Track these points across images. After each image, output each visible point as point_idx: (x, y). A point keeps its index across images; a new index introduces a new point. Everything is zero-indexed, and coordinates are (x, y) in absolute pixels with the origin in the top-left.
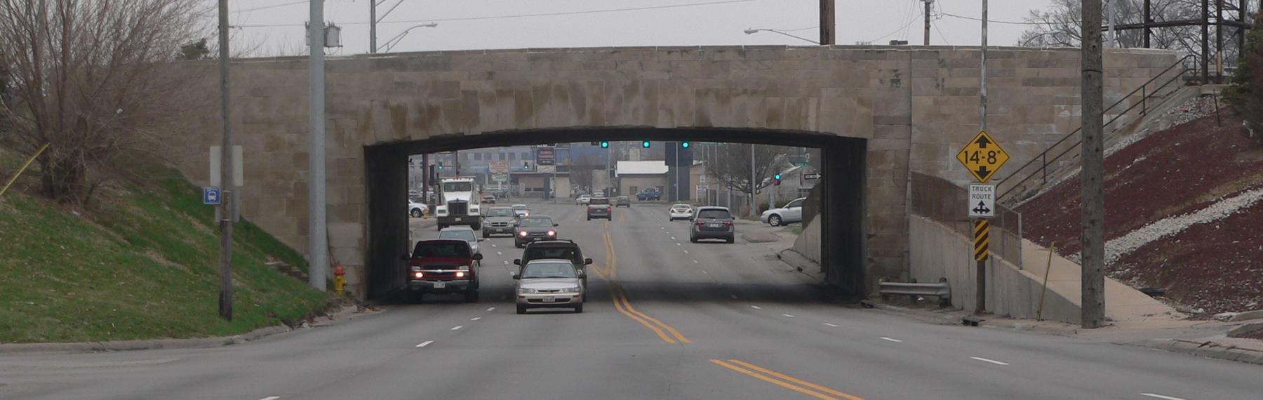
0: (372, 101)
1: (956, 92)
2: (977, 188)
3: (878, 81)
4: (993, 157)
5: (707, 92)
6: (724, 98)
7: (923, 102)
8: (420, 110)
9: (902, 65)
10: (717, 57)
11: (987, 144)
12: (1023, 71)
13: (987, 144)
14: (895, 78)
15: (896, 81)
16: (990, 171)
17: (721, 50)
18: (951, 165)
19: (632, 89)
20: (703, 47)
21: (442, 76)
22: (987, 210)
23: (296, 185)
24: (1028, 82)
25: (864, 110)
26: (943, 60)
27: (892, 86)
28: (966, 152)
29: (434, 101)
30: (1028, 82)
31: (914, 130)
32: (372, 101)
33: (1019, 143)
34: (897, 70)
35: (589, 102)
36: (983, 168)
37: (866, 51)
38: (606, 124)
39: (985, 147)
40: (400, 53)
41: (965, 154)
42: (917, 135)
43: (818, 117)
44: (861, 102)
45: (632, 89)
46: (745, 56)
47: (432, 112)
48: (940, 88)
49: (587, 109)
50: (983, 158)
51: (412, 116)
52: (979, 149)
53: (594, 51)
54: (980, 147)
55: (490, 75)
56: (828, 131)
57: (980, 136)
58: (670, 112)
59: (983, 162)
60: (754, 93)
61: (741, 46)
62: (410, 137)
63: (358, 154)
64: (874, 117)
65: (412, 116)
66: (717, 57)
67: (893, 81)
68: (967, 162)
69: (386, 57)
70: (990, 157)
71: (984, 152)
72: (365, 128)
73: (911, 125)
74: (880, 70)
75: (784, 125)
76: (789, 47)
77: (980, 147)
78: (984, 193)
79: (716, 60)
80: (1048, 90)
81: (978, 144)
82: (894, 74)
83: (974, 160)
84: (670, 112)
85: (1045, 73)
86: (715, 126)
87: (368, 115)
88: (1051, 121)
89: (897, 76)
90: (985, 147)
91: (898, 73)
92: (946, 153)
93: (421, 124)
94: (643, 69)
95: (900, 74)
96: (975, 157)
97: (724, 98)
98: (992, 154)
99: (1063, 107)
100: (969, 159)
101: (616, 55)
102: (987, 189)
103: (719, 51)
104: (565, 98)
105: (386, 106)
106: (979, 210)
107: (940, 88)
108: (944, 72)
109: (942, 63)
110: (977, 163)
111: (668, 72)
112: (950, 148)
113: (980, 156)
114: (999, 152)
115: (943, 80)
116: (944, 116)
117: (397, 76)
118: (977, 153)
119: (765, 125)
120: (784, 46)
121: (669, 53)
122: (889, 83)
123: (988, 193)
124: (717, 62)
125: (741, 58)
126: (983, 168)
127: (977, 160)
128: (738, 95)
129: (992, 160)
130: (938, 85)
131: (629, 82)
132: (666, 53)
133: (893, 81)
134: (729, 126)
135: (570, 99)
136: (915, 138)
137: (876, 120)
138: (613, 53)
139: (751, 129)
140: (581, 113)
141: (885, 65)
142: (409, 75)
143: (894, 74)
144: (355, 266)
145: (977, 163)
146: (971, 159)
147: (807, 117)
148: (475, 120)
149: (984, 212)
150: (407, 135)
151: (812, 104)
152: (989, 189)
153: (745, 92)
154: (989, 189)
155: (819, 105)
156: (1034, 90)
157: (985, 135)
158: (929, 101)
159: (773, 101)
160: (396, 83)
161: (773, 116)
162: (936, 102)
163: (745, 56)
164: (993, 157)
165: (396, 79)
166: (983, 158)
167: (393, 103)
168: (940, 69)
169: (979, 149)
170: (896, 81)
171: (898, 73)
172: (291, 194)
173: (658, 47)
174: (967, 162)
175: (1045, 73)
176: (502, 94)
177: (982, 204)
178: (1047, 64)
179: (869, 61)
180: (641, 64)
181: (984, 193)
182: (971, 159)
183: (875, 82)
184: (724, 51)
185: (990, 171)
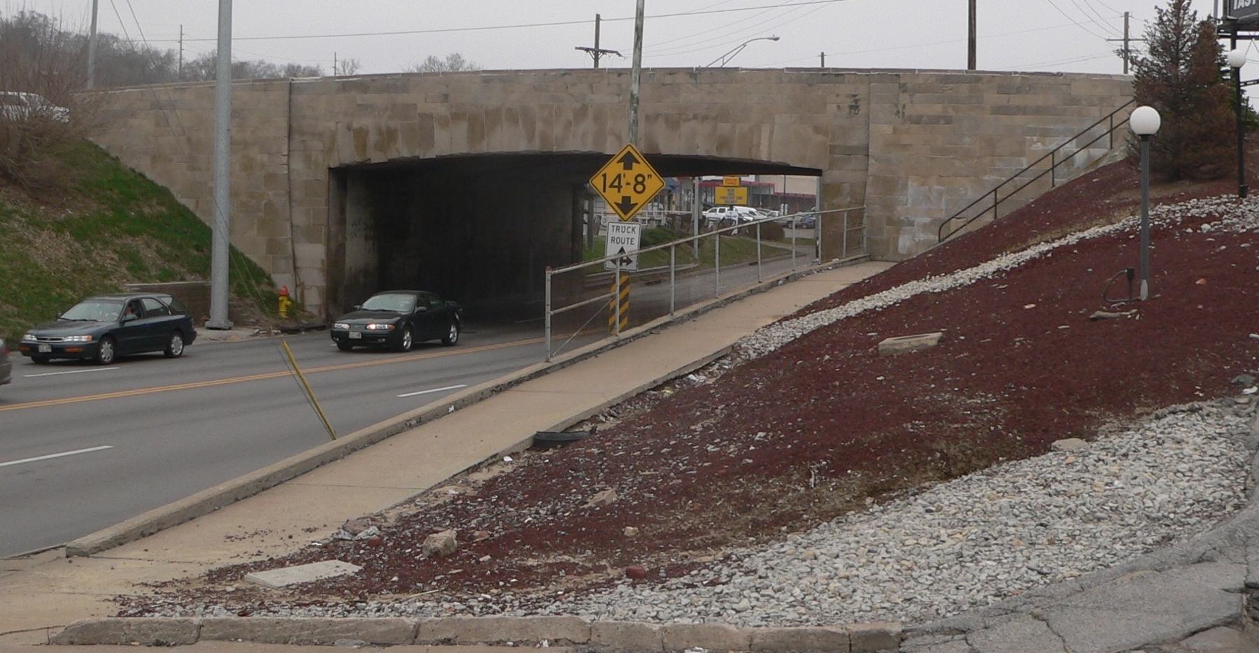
0: (337, 123)
1: (918, 120)
2: (618, 229)
3: (835, 106)
4: (642, 183)
5: (657, 116)
6: (673, 124)
7: (882, 130)
8: (380, 132)
9: (862, 90)
10: (668, 80)
11: (634, 164)
12: (992, 98)
13: (634, 164)
14: (854, 104)
15: (855, 108)
16: (636, 204)
17: (672, 72)
18: (910, 200)
19: (581, 113)
20: (653, 69)
21: (402, 98)
22: (629, 261)
23: (265, 205)
24: (998, 110)
25: (819, 138)
26: (904, 84)
27: (850, 113)
28: (604, 176)
29: (394, 124)
30: (998, 110)
31: (871, 161)
32: (337, 123)
33: (986, 178)
34: (856, 96)
35: (539, 126)
36: (626, 199)
37: (823, 75)
38: (555, 149)
39: (630, 168)
40: (364, 76)
41: (603, 178)
42: (874, 166)
43: (770, 146)
44: (817, 129)
45: (581, 113)
46: (696, 79)
47: (389, 136)
48: (901, 115)
49: (537, 134)
50: (628, 184)
51: (372, 138)
52: (622, 172)
53: (545, 73)
54: (625, 168)
55: (446, 97)
56: (780, 160)
57: (625, 152)
58: (619, 138)
59: (627, 191)
60: (705, 118)
61: (692, 68)
62: (370, 159)
63: (323, 176)
64: (830, 146)
65: (372, 138)
66: (668, 80)
67: (851, 107)
68: (604, 191)
69: (351, 79)
70: (638, 183)
71: (630, 176)
72: (329, 151)
73: (868, 155)
74: (838, 96)
75: (735, 153)
76: (743, 69)
77: (625, 168)
78: (626, 235)
79: (666, 82)
80: (1019, 119)
81: (622, 164)
82: (852, 99)
83: (615, 187)
84: (619, 138)
85: (1016, 100)
86: (664, 153)
87: (333, 138)
88: (1022, 154)
89: (856, 101)
90: (630, 168)
91: (858, 97)
92: (905, 186)
93: (381, 147)
94: (592, 92)
95: (859, 100)
96: (616, 184)
97: (673, 124)
98: (640, 179)
99: (1035, 138)
100: (608, 183)
101: (566, 76)
102: (630, 230)
103: (670, 74)
104: (516, 122)
105: (349, 129)
106: (625, 261)
107: (901, 115)
108: (904, 98)
109: (903, 88)
110: (619, 191)
111: (619, 95)
112: (910, 183)
113: (623, 183)
114: (650, 176)
115: (904, 106)
116: (905, 147)
117: (360, 98)
118: (619, 176)
119: (714, 153)
120: (737, 69)
121: (619, 75)
122: (848, 110)
123: (631, 236)
124: (666, 84)
125: (693, 81)
126: (626, 199)
127: (619, 187)
128: (688, 120)
129: (639, 188)
130: (898, 112)
131: (578, 106)
132: (616, 75)
133: (851, 107)
134: (669, 153)
135: (520, 121)
136: (871, 170)
137: (832, 149)
138: (564, 75)
139: (701, 157)
140: (530, 138)
141: (845, 89)
142: (371, 98)
143: (852, 99)
144: (317, 287)
145: (619, 191)
146: (611, 186)
147: (759, 145)
148: (429, 140)
149: (624, 264)
150: (368, 157)
151: (765, 130)
152: (633, 230)
153: (695, 117)
154: (633, 230)
155: (772, 132)
156: (1005, 120)
157: (632, 151)
158: (887, 129)
159: (724, 128)
160: (359, 105)
161: (723, 143)
162: (895, 131)
163: (696, 79)
164: (642, 183)
165: (359, 102)
166: (628, 184)
167: (356, 125)
168: (901, 95)
169: (622, 172)
170: (855, 108)
171: (858, 97)
172: (261, 214)
173: (609, 69)
174: (604, 191)
175: (1016, 100)
176: (456, 117)
177: (622, 250)
178: (1019, 91)
179: (826, 85)
180: (591, 87)
181: (626, 235)
182: (611, 186)
183: (832, 108)
184: (674, 74)
185: (636, 204)
